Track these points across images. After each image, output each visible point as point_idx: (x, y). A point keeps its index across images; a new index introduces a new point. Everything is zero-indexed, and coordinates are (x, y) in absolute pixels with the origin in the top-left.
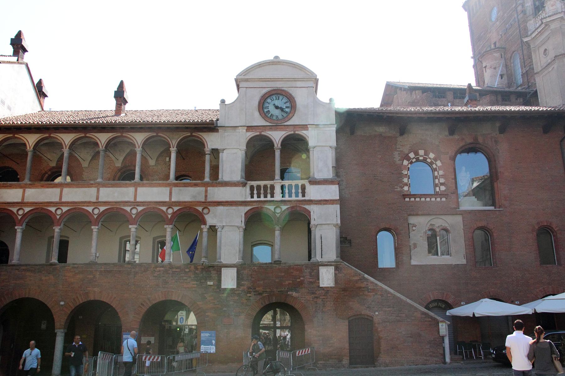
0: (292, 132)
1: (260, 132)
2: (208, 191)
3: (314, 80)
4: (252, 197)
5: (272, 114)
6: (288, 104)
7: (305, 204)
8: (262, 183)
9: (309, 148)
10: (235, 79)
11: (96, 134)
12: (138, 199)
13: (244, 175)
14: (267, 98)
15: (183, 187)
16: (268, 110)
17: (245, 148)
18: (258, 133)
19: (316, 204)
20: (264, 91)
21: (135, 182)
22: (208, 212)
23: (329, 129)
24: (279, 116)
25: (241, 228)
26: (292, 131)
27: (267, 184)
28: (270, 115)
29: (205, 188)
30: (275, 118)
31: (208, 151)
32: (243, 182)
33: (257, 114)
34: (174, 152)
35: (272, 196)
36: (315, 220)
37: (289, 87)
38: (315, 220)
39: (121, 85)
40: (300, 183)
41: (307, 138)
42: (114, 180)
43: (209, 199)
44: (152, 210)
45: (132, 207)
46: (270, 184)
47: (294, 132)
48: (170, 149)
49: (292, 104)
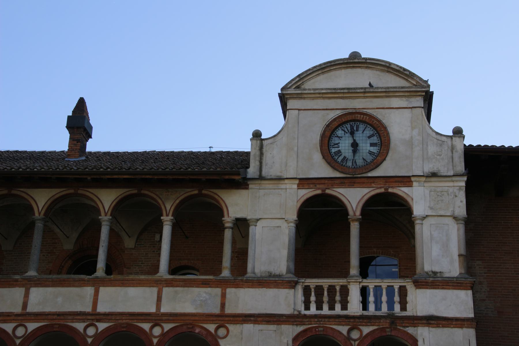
0: (382, 190)
1: (324, 190)
2: (228, 296)
3: (424, 94)
4: (307, 308)
5: (345, 157)
6: (375, 140)
7: (407, 325)
8: (325, 282)
9: (413, 219)
10: (279, 94)
11: (29, 191)
12: (101, 309)
13: (292, 267)
14: (337, 128)
15: (181, 287)
16: (337, 149)
17: (295, 217)
18: (319, 192)
20: (333, 115)
21: (97, 278)
22: (226, 333)
23: (451, 184)
24: (358, 164)
26: (381, 188)
27: (333, 284)
28: (341, 158)
29: (222, 290)
30: (351, 164)
31: (228, 222)
32: (290, 279)
33: (317, 156)
34: (168, 223)
35: (344, 307)
37: (377, 108)
39: (81, 104)
40: (397, 284)
41: (409, 200)
42: (59, 273)
43: (229, 310)
44: (125, 329)
45: (88, 323)
46: (341, 284)
47: (385, 189)
48: (162, 218)
49: (383, 139)
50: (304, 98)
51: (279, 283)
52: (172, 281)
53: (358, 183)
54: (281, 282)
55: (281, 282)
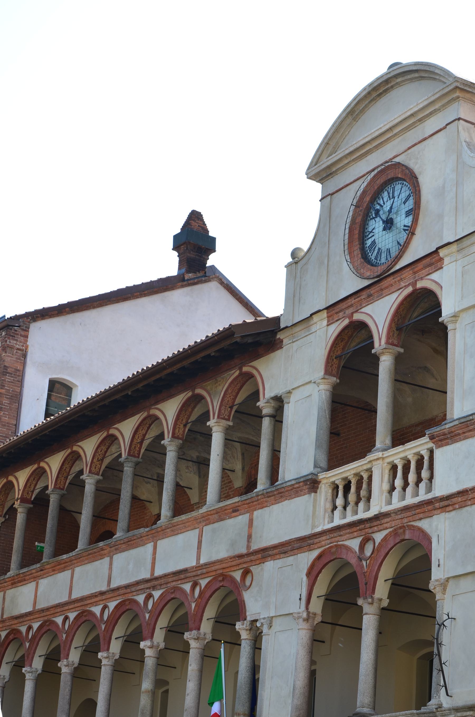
0: (410, 289)
7: (421, 515)
18: (346, 322)
19: (444, 509)
20: (362, 185)
25: (299, 618)
27: (358, 471)
36: (439, 566)
37: (409, 148)
38: (439, 566)
46: (365, 467)
50: (335, 173)
51: (298, 488)
52: (208, 515)
53: (387, 288)
54: (297, 485)
55: (297, 485)
